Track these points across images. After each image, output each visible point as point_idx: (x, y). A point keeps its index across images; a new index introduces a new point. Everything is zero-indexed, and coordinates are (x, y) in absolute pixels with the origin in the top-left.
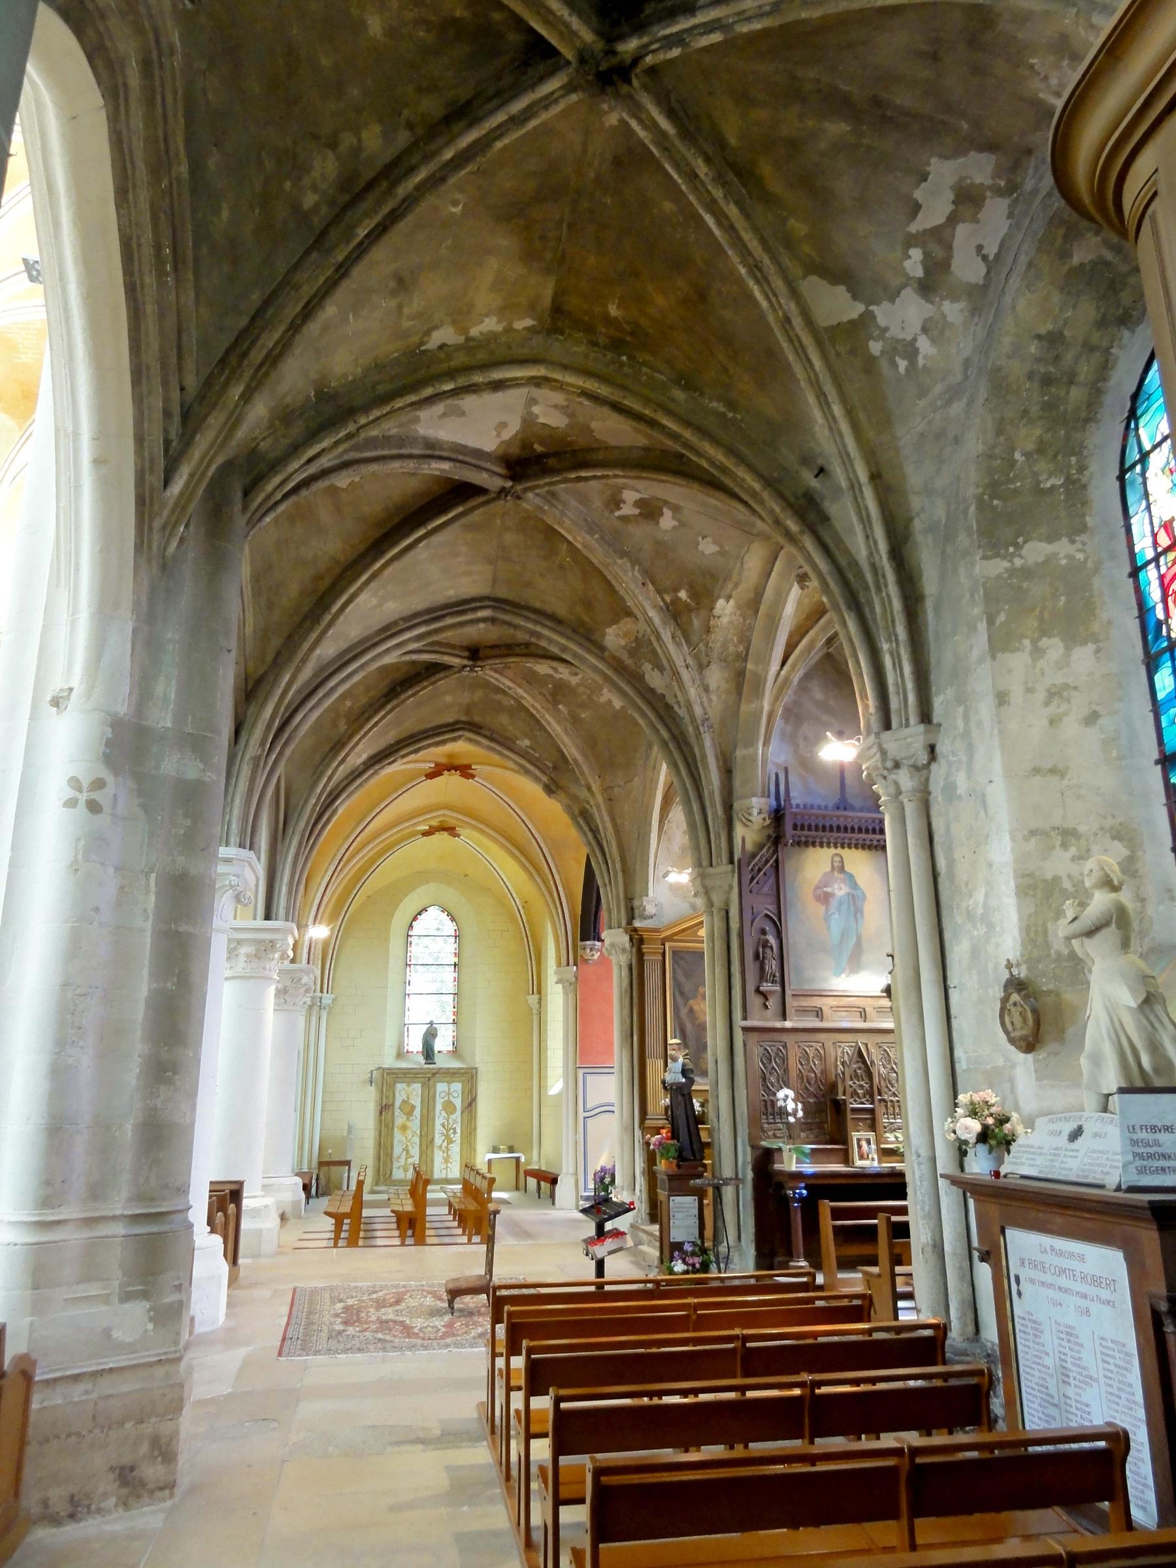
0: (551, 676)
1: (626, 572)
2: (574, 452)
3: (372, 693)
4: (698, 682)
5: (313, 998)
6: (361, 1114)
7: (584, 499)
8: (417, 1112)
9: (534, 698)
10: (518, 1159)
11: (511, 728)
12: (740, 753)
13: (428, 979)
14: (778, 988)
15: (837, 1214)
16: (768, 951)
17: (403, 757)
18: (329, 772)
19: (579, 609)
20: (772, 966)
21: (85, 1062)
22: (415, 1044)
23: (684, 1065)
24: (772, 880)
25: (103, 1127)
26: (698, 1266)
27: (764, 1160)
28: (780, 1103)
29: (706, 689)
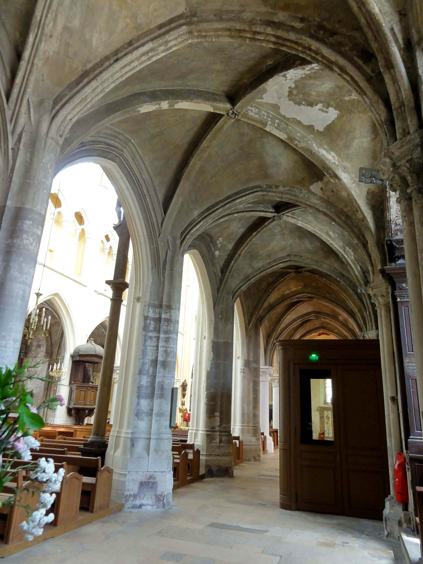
21: (246, 406)
25: (248, 414)
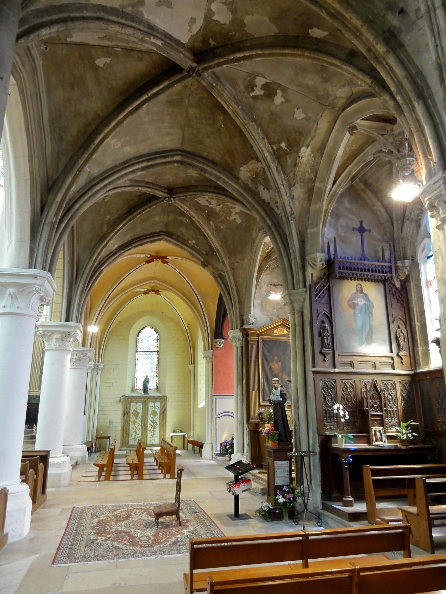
0: (207, 206)
1: (254, 130)
2: (233, 44)
3: (120, 212)
4: (288, 194)
5: (94, 365)
6: (115, 416)
7: (234, 84)
8: (140, 415)
9: (198, 217)
10: (184, 436)
11: (186, 235)
12: (309, 231)
13: (145, 358)
14: (331, 351)
15: (375, 473)
16: (326, 332)
17: (135, 247)
18: (99, 251)
19: (227, 157)
20: (328, 340)
22: (139, 385)
23: (281, 391)
24: (327, 296)
26: (292, 499)
27: (326, 442)
28: (335, 412)
29: (293, 198)
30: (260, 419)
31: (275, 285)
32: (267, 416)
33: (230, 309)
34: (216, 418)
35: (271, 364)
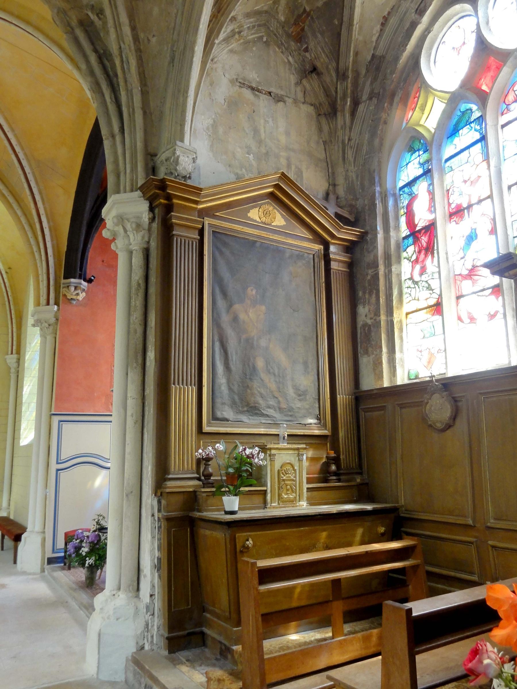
30: (199, 479)
31: (253, 89)
32: (228, 467)
33: (113, 136)
34: (58, 470)
35: (237, 307)
